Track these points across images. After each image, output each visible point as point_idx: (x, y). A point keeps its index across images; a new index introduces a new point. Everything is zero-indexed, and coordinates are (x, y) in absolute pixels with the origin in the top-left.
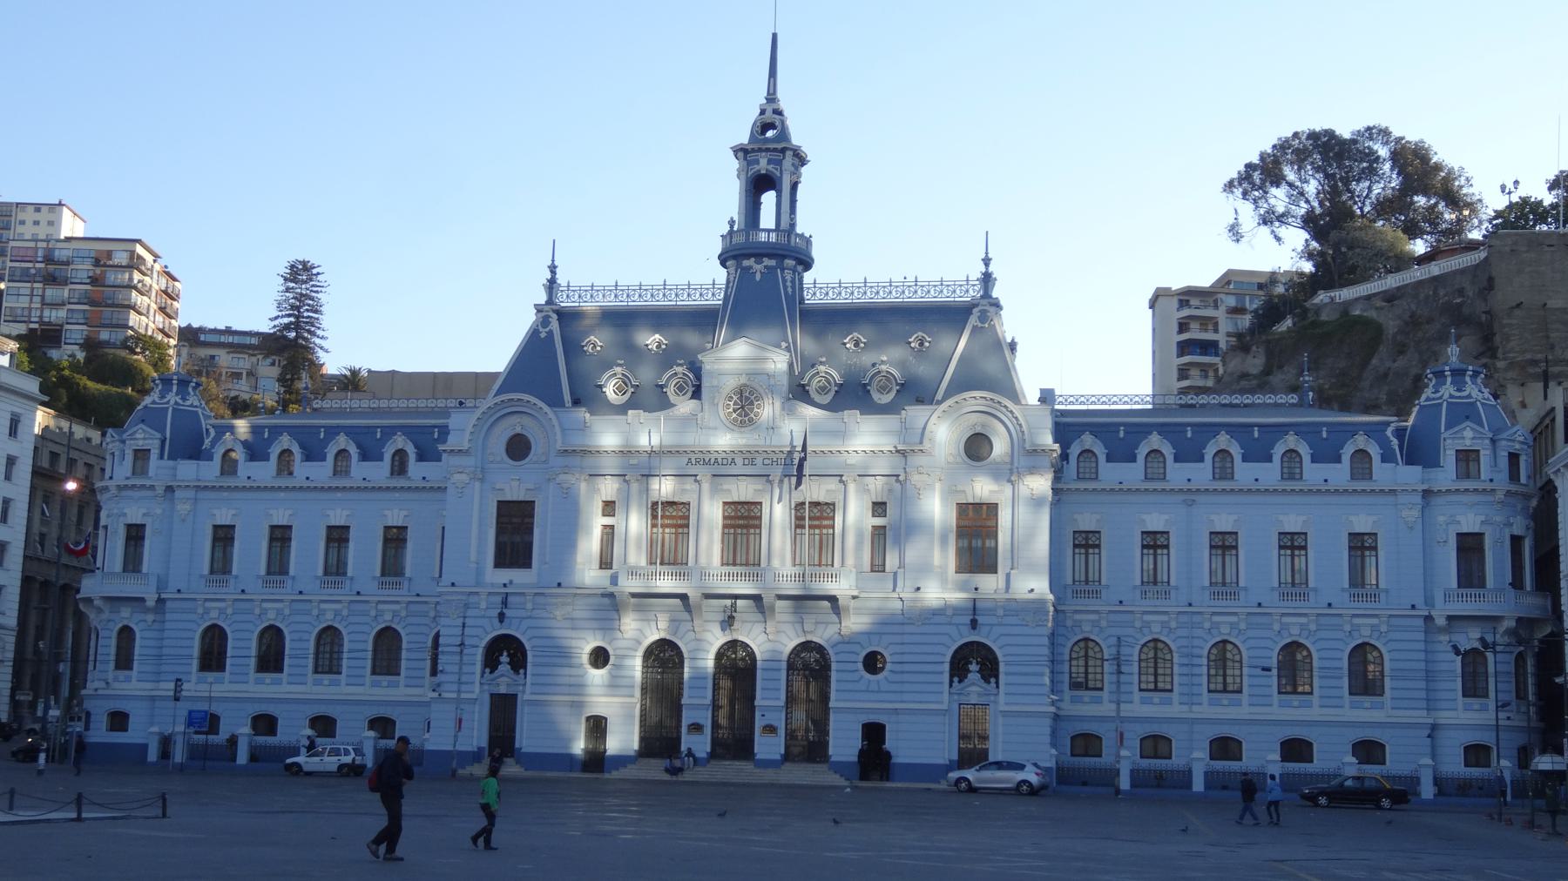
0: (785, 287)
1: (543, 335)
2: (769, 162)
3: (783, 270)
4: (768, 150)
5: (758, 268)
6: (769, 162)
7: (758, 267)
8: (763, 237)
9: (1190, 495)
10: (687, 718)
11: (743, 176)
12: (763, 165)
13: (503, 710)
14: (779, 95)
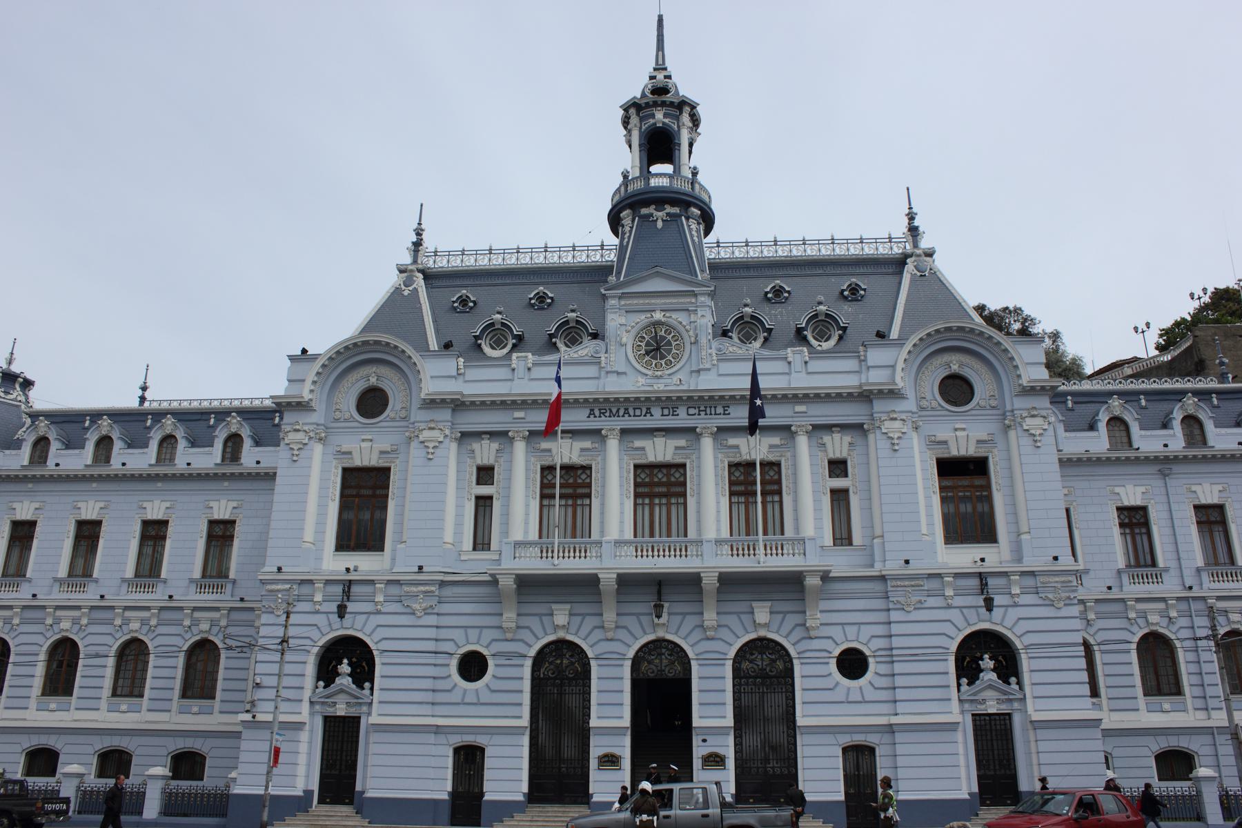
1: (406, 293)
2: (665, 116)
4: (663, 104)
6: (660, 125)
7: (660, 214)
9: (1164, 463)
10: (597, 749)
12: (659, 116)
14: (667, 64)
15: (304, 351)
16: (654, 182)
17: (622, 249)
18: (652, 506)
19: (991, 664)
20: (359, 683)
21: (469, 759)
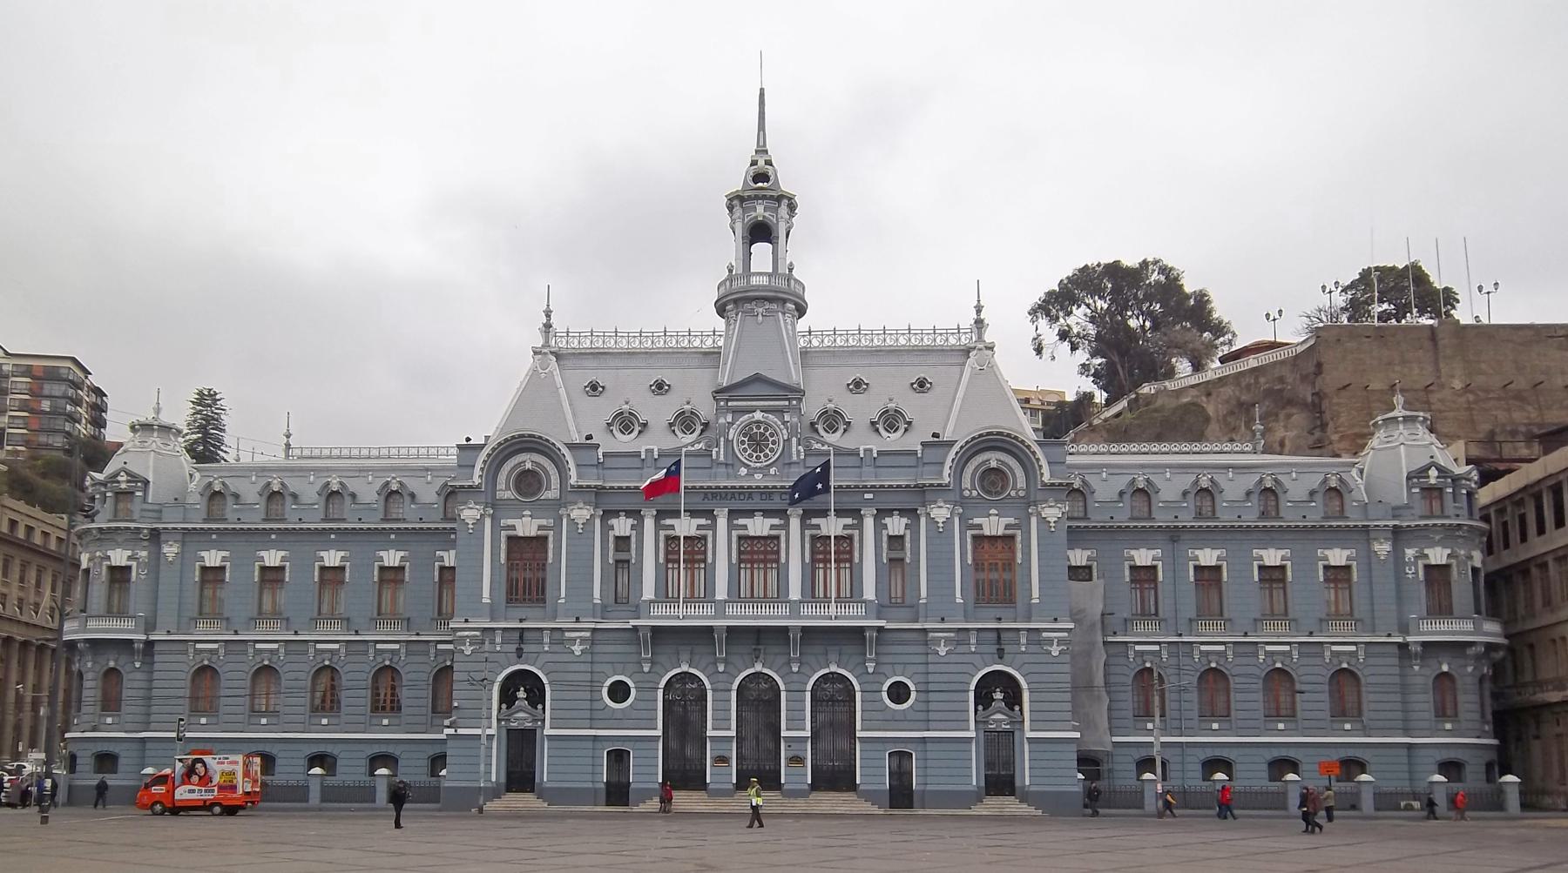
8: (764, 281)
11: (739, 226)
13: (521, 745)
15: (468, 439)
16: (755, 281)
17: (728, 337)
18: (752, 569)
20: (533, 705)
21: (618, 758)
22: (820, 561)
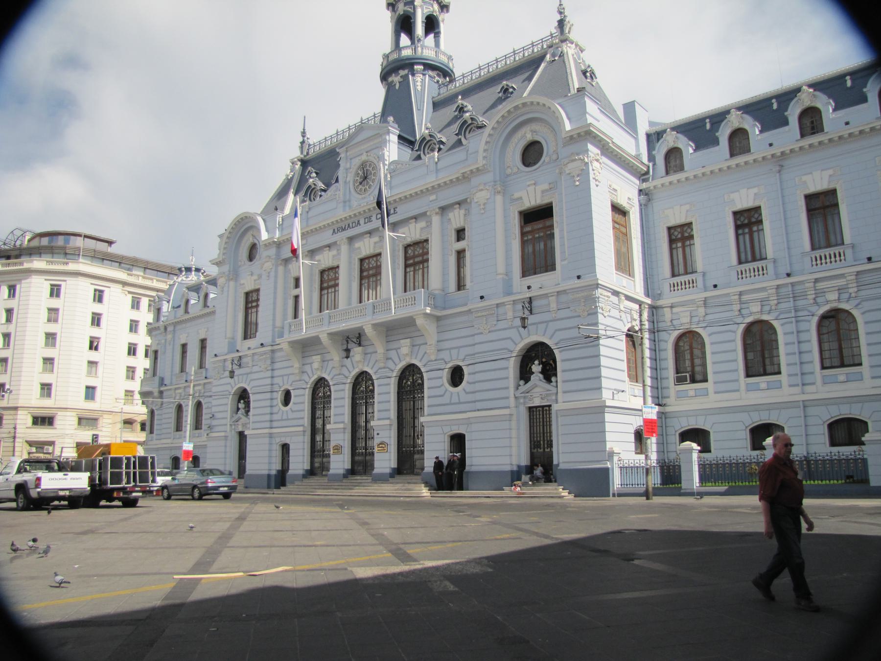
0: (415, 86)
3: (413, 75)
5: (395, 79)
19: (540, 368)
22: (410, 265)
